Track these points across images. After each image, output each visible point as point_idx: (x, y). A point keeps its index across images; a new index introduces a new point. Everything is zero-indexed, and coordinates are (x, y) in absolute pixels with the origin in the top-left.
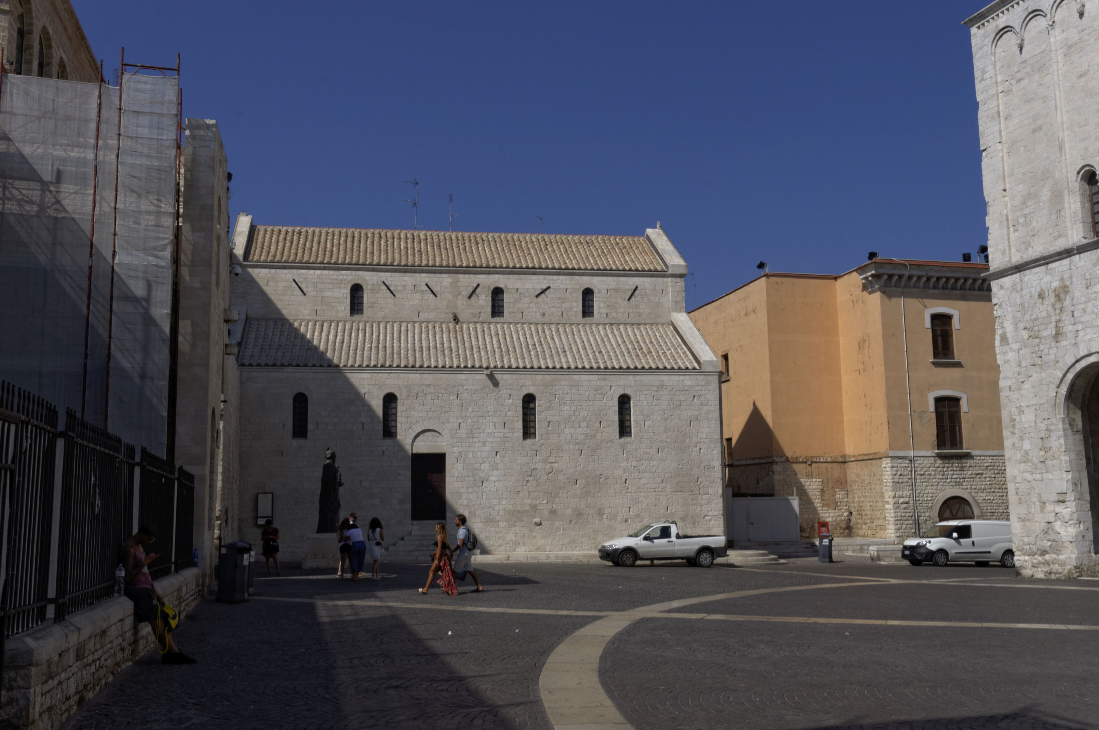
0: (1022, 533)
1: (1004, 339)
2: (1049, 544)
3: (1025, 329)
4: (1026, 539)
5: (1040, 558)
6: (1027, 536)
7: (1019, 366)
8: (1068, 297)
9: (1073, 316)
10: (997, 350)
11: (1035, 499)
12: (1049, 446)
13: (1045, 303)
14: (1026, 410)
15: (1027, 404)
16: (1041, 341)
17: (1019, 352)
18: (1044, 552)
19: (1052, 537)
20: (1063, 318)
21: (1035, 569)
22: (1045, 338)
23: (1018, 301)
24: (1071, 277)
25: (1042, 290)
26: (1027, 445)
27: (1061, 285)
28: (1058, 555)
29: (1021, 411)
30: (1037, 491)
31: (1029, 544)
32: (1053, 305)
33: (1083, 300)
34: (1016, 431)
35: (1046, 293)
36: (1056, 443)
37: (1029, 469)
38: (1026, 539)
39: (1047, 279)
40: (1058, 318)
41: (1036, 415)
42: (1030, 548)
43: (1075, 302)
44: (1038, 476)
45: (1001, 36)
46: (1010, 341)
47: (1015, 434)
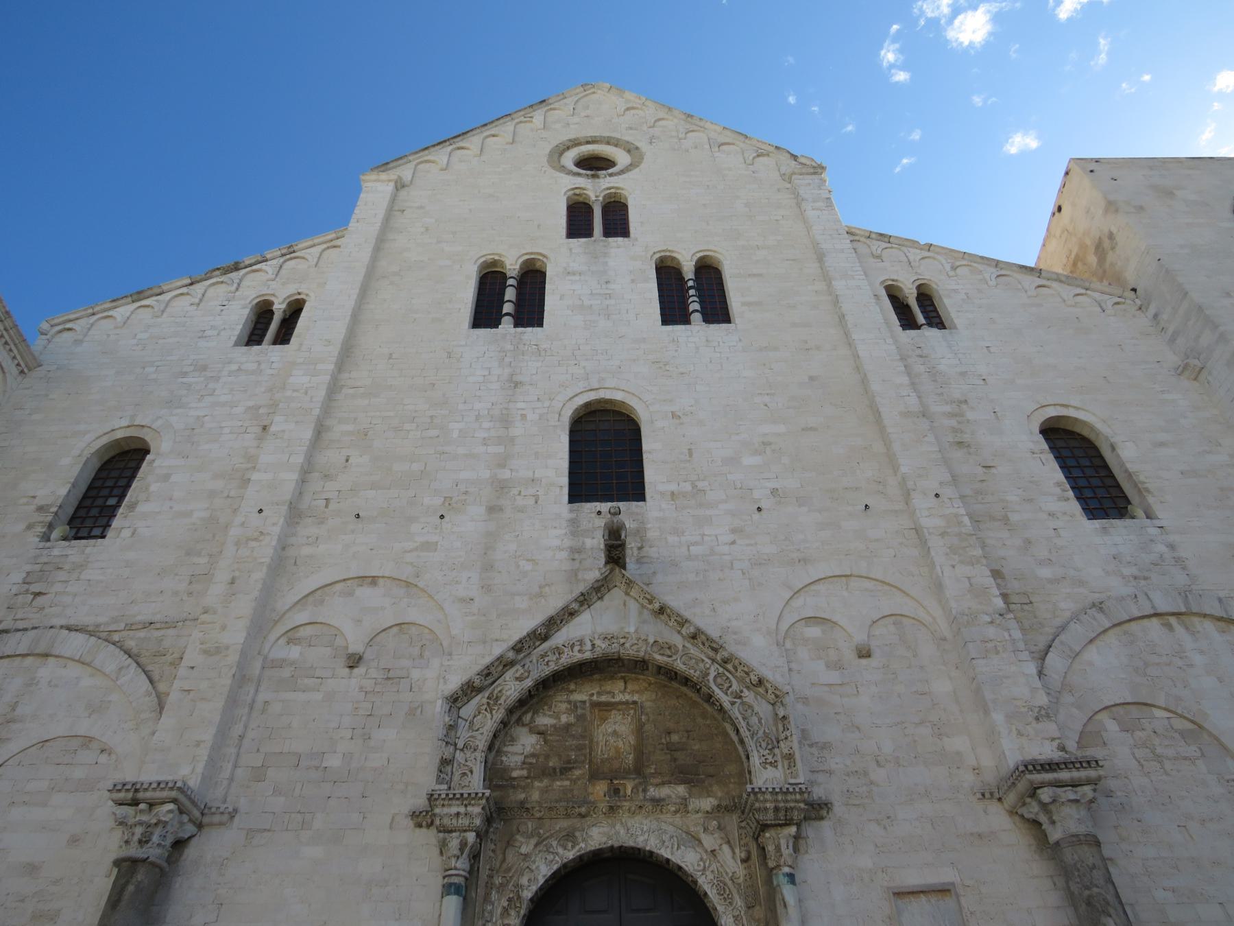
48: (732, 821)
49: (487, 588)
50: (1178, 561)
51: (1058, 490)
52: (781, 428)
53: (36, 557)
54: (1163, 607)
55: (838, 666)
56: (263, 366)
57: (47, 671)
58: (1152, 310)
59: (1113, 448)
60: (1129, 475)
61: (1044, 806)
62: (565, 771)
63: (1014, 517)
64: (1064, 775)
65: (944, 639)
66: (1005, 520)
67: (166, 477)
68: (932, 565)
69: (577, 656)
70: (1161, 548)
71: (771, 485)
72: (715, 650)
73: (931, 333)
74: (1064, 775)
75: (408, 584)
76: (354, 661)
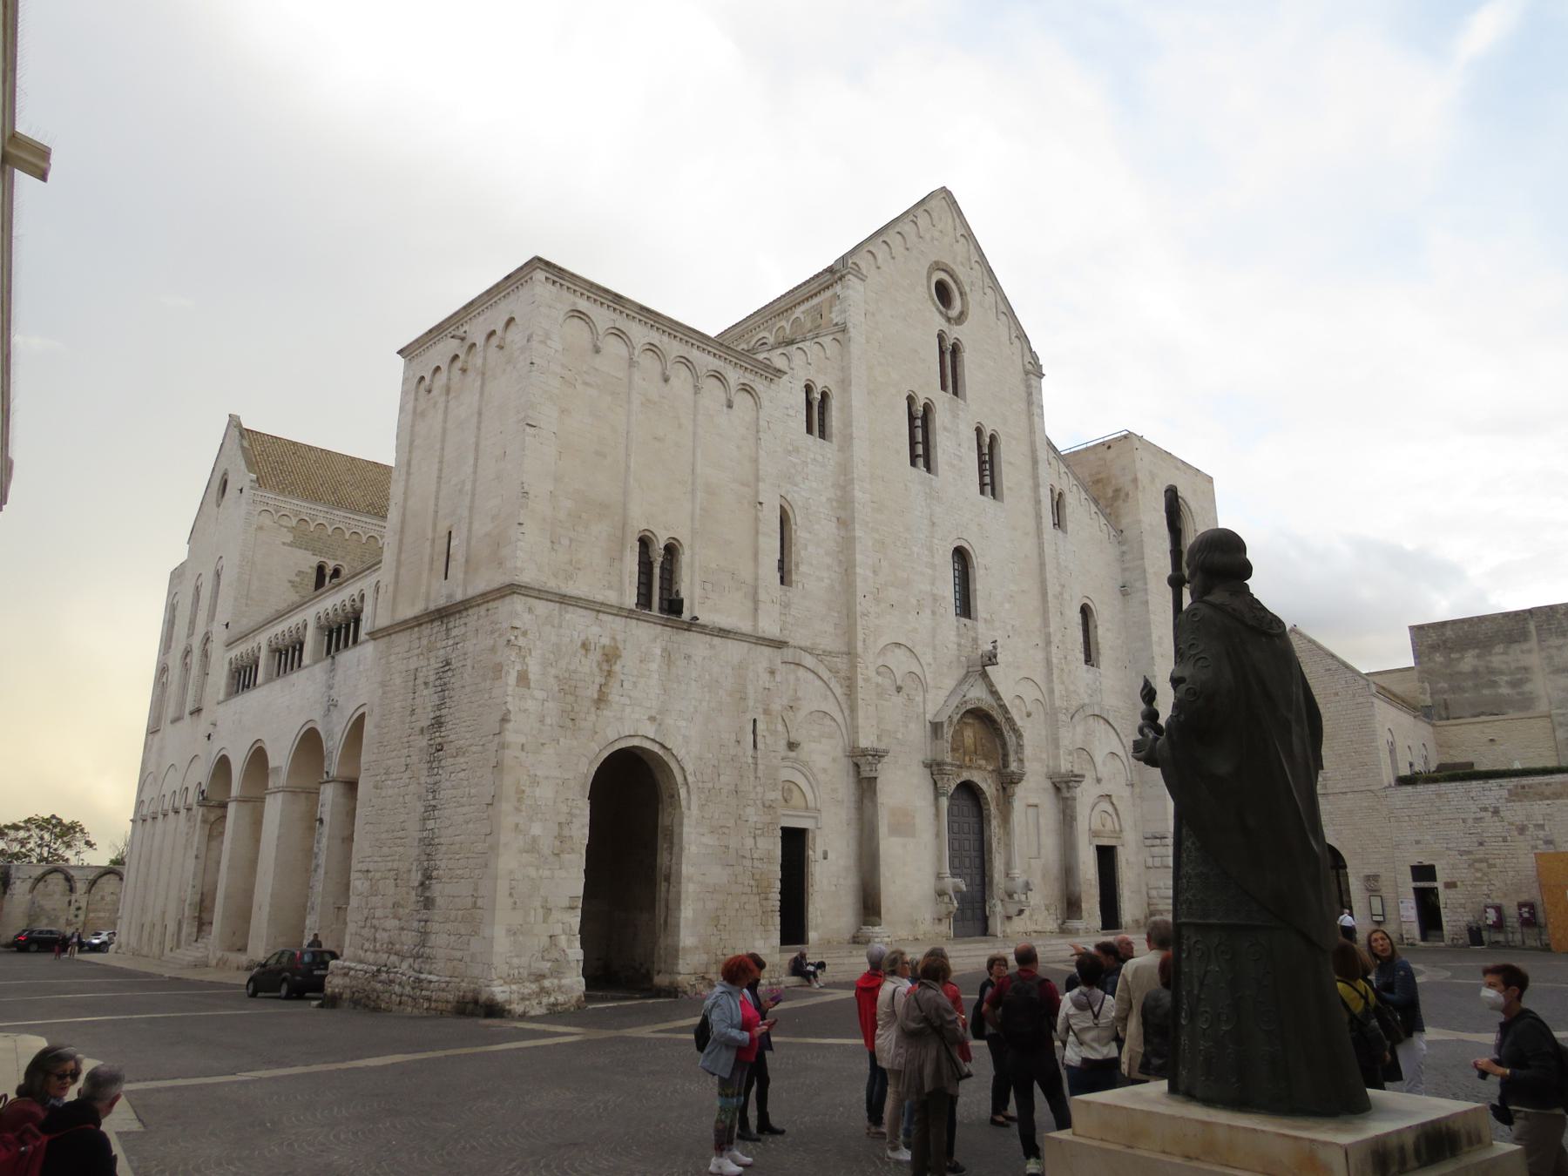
0: (511, 952)
1: (523, 679)
2: (549, 965)
3: (556, 677)
4: (515, 961)
5: (534, 987)
6: (517, 956)
7: (540, 721)
8: (618, 662)
9: (622, 686)
10: (510, 690)
11: (538, 904)
12: (568, 835)
17: (543, 704)
19: (555, 954)
20: (610, 684)
21: (527, 1003)
23: (554, 639)
24: (625, 641)
25: (587, 639)
27: (613, 644)
28: (560, 979)
29: (535, 781)
31: (518, 968)
32: (599, 664)
34: (523, 807)
35: (592, 647)
38: (515, 961)
39: (595, 629)
40: (603, 681)
41: (557, 792)
42: (519, 973)
43: (625, 671)
44: (547, 873)
45: (573, 316)
46: (532, 685)
47: (521, 811)
49: (935, 659)
54: (1096, 713)
55: (1022, 719)
56: (826, 460)
57: (801, 672)
59: (1096, 627)
60: (1097, 644)
62: (959, 749)
64: (1077, 779)
65: (1047, 713)
67: (805, 548)
70: (1098, 683)
72: (1006, 713)
73: (1060, 533)
74: (1077, 779)
75: (911, 650)
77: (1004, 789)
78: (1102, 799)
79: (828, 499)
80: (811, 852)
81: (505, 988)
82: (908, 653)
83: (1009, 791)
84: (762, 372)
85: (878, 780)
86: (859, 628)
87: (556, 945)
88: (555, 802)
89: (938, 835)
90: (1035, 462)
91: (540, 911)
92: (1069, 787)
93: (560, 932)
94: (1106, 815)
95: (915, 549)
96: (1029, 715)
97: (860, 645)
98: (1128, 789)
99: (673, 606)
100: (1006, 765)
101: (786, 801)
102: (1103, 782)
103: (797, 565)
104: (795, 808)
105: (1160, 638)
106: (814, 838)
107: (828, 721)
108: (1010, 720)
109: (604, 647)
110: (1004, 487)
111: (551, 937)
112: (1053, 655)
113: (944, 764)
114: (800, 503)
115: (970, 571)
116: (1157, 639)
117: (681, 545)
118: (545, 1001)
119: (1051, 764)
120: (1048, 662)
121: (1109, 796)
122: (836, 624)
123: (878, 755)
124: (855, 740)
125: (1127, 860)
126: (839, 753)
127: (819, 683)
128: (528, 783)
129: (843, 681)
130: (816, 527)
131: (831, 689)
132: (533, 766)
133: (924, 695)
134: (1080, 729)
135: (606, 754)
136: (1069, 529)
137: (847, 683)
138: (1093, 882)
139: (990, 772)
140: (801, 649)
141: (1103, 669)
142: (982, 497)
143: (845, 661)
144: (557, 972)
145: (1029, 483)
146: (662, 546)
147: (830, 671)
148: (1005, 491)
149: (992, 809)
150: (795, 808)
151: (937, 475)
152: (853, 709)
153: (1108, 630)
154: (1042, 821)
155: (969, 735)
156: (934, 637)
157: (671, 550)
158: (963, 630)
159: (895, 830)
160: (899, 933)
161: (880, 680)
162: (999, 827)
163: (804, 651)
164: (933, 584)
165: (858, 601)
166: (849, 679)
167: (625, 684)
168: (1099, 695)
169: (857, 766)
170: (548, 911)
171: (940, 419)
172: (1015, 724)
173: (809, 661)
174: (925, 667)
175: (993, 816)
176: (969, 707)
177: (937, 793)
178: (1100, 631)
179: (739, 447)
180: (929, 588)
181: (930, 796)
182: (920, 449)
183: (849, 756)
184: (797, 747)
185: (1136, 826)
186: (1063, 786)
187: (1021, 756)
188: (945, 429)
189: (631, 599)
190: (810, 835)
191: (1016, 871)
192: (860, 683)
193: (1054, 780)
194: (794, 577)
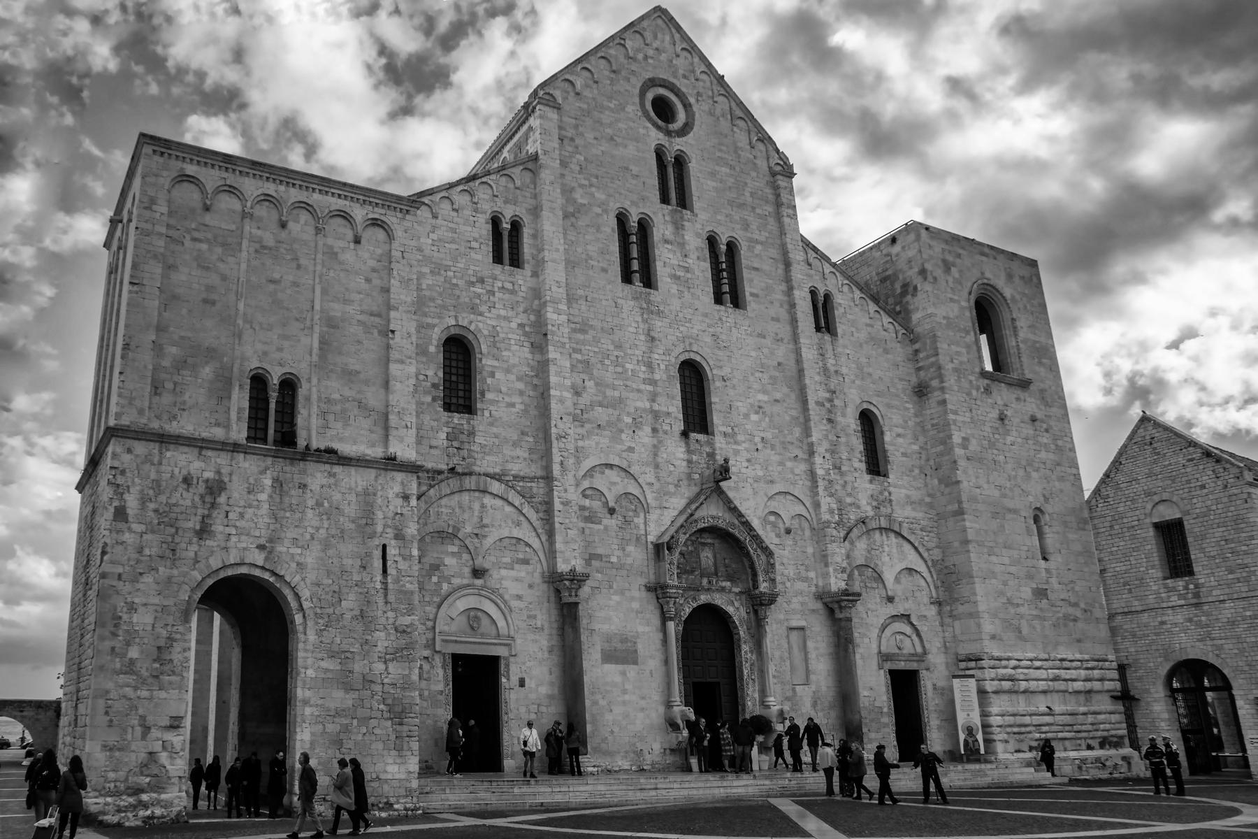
0: (106, 766)
2: (148, 780)
3: (156, 511)
4: (112, 775)
5: (131, 800)
8: (223, 494)
13: (190, 490)
14: (141, 609)
15: (144, 601)
16: (177, 532)
18: (138, 791)
20: (214, 515)
21: (123, 815)
22: (184, 530)
24: (231, 474)
25: (189, 474)
26: (134, 653)
28: (160, 793)
29: (132, 608)
30: (141, 711)
32: (202, 497)
33: (242, 503)
36: (180, 656)
37: (133, 683)
38: (112, 775)
40: (206, 512)
41: (156, 618)
48: (744, 597)
49: (658, 478)
50: (891, 501)
51: (859, 456)
52: (765, 398)
53: (448, 423)
54: (883, 525)
55: (778, 536)
56: (516, 287)
57: (488, 500)
58: (917, 346)
59: (882, 433)
60: (885, 451)
61: (841, 607)
62: (692, 572)
63: (844, 468)
66: (840, 468)
67: (492, 375)
68: (817, 494)
69: (703, 525)
70: (886, 494)
71: (762, 434)
73: (827, 337)
75: (626, 471)
76: (612, 511)
77: (756, 612)
78: (896, 618)
79: (519, 325)
80: (504, 680)
81: (101, 800)
82: (623, 474)
83: (761, 613)
84: (396, 205)
85: (580, 607)
86: (555, 451)
87: (156, 762)
88: (153, 627)
89: (666, 662)
90: (787, 265)
91: (138, 730)
92: (841, 607)
93: (160, 749)
94: (902, 637)
95: (628, 366)
96: (788, 531)
97: (556, 470)
98: (932, 611)
99: (287, 438)
100: (756, 586)
101: (472, 628)
102: (897, 599)
103: (483, 394)
104: (483, 635)
105: (965, 439)
106: (507, 666)
107: (522, 547)
108: (756, 538)
109: (207, 481)
110: (747, 294)
111: (150, 753)
112: (818, 466)
113: (667, 587)
114: (486, 332)
115: (705, 383)
116: (960, 441)
117: (299, 380)
118: (142, 813)
119: (820, 584)
120: (812, 475)
121: (908, 616)
122: (530, 449)
123: (577, 580)
124: (555, 565)
125: (934, 685)
126: (537, 579)
127: (508, 509)
128: (125, 609)
129: (540, 507)
130: (504, 353)
131: (524, 515)
132: (130, 593)
133: (645, 518)
134: (861, 545)
135: (210, 582)
136: (839, 331)
137: (544, 508)
138: (885, 710)
139: (736, 594)
140: (487, 475)
141: (892, 477)
142: (718, 307)
143: (542, 485)
144: (158, 786)
145: (783, 287)
146: (276, 381)
147: (524, 497)
148: (748, 298)
149: (741, 633)
150: (483, 635)
151: (656, 289)
152: (551, 534)
153: (899, 435)
154: (810, 644)
155: (707, 556)
156: (656, 455)
157: (289, 386)
158: (694, 446)
159: (610, 657)
160: (620, 763)
161: (587, 503)
162: (751, 652)
163: (491, 478)
164: (653, 401)
165: (553, 423)
166: (546, 503)
167: (231, 515)
168: (888, 505)
169: (558, 591)
170: (146, 729)
171: (661, 230)
172: (762, 542)
173: (496, 487)
174: (645, 487)
175: (743, 640)
176: (701, 525)
177: (664, 619)
178: (887, 438)
179: (368, 280)
180: (647, 405)
181: (656, 620)
182: (635, 265)
183: (549, 582)
184: (483, 575)
185: (946, 647)
186: (836, 606)
187: (772, 576)
188: (667, 242)
189: (239, 433)
190: (503, 663)
191: (772, 699)
192: (557, 505)
193: (825, 600)
194: (479, 405)
